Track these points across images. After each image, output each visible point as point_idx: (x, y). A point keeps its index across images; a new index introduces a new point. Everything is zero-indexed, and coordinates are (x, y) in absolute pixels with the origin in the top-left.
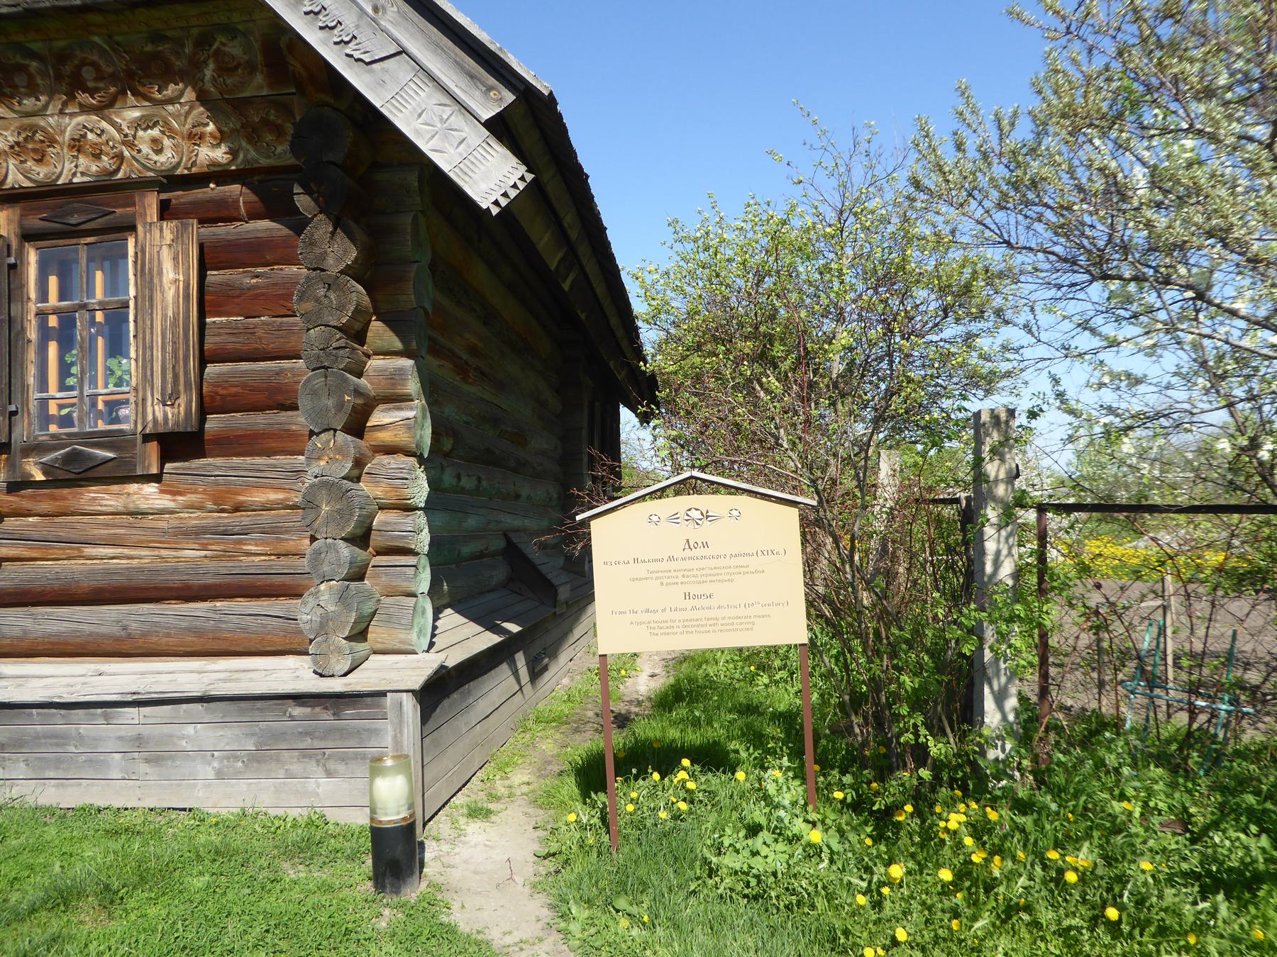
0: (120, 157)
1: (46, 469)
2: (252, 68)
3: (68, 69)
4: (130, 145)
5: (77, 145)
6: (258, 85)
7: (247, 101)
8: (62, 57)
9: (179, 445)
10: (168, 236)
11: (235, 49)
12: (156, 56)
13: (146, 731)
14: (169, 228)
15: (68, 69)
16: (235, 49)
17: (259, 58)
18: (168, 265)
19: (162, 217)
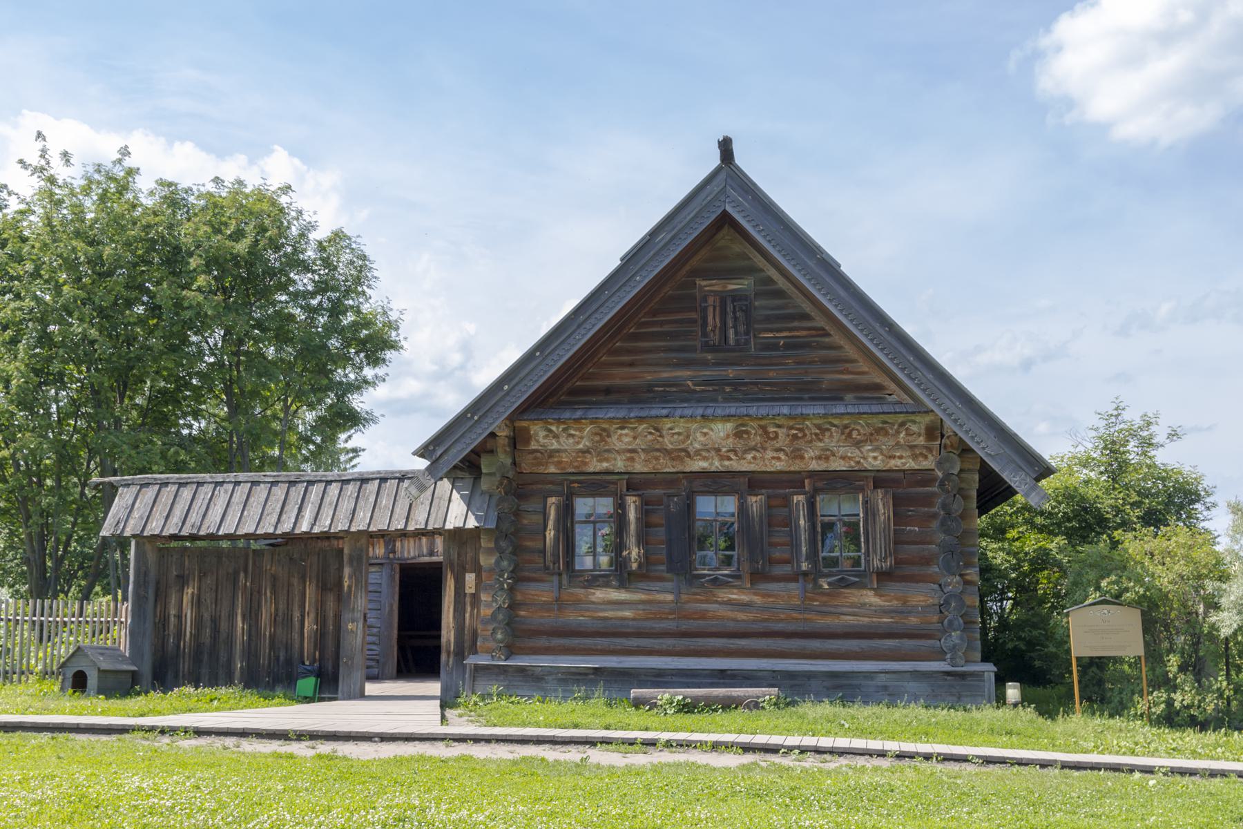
0: (858, 462)
1: (829, 584)
2: (919, 435)
3: (847, 431)
4: (864, 458)
5: (843, 458)
6: (921, 441)
7: (915, 446)
8: (846, 427)
9: (885, 576)
10: (880, 496)
11: (914, 428)
12: (882, 429)
13: (888, 684)
14: (880, 493)
15: (847, 431)
16: (914, 428)
17: (923, 431)
18: (881, 506)
19: (875, 487)
